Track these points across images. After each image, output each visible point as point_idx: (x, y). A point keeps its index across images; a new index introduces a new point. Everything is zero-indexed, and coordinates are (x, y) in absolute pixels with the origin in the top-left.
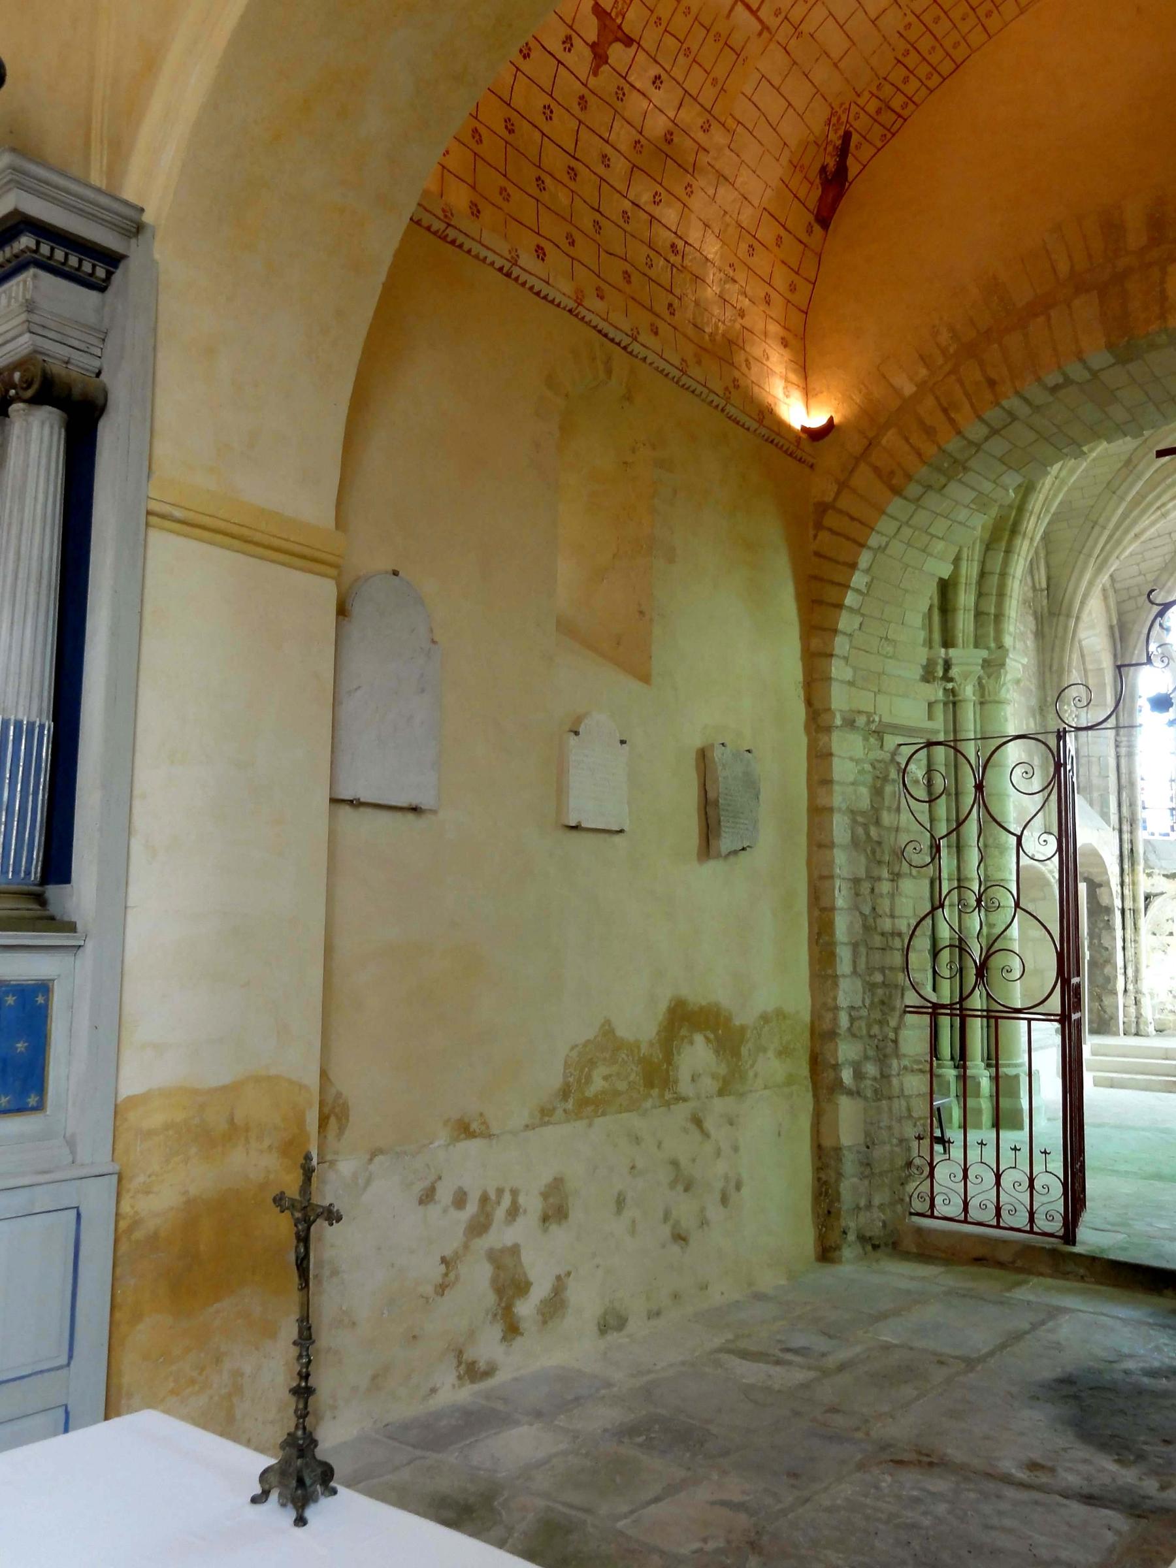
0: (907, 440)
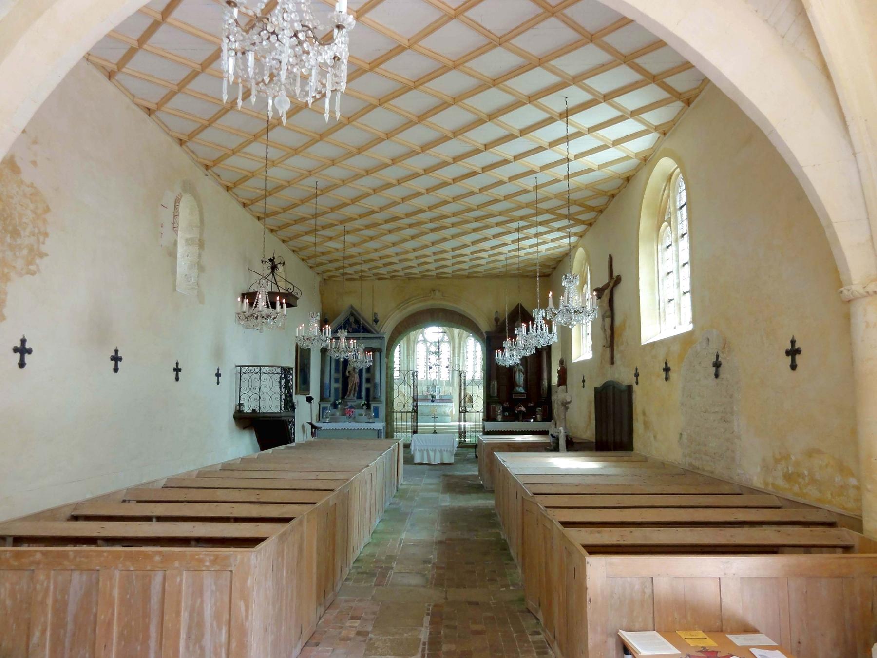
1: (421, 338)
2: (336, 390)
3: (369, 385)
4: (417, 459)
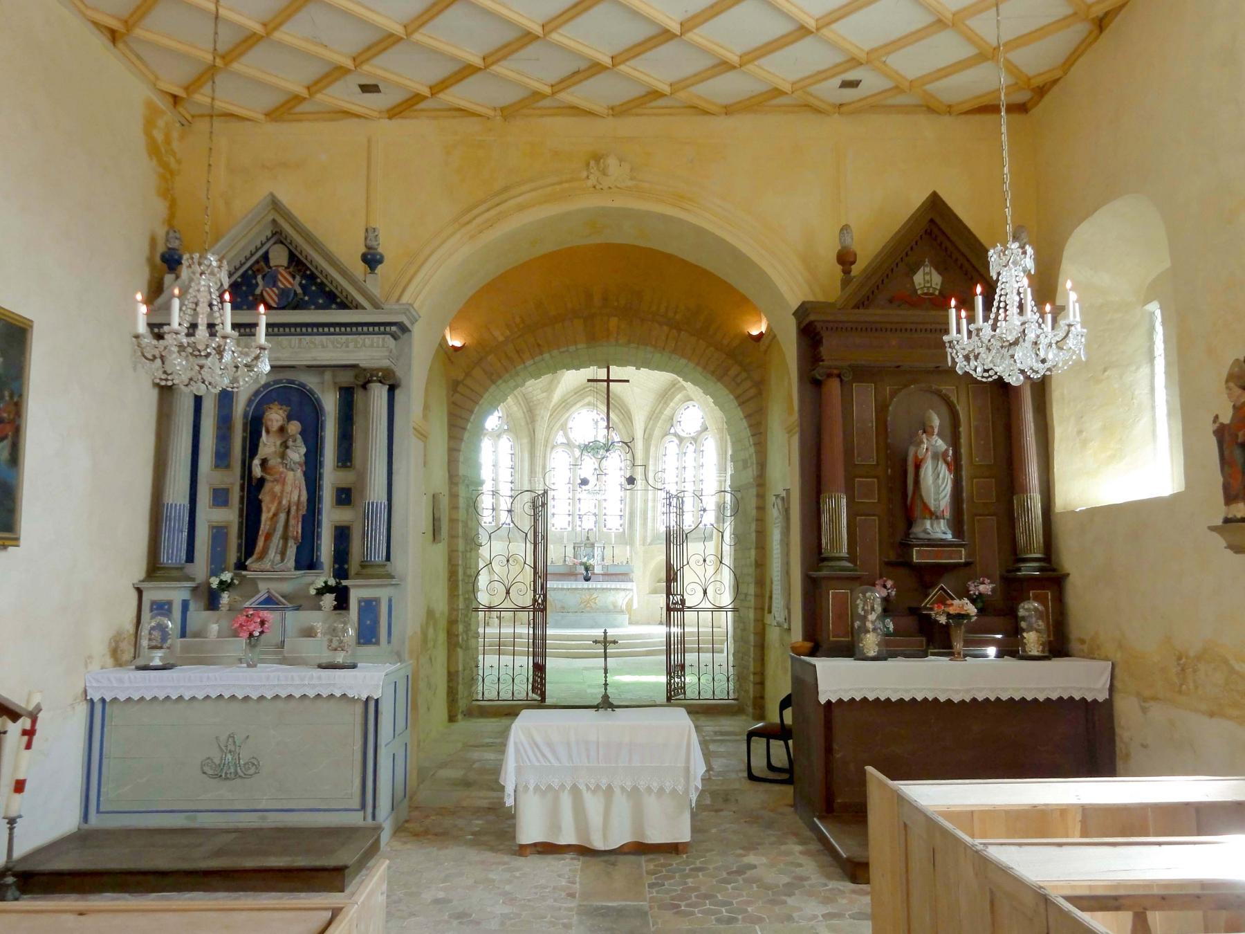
1: (560, 438)
2: (219, 533)
3: (344, 516)
4: (531, 831)
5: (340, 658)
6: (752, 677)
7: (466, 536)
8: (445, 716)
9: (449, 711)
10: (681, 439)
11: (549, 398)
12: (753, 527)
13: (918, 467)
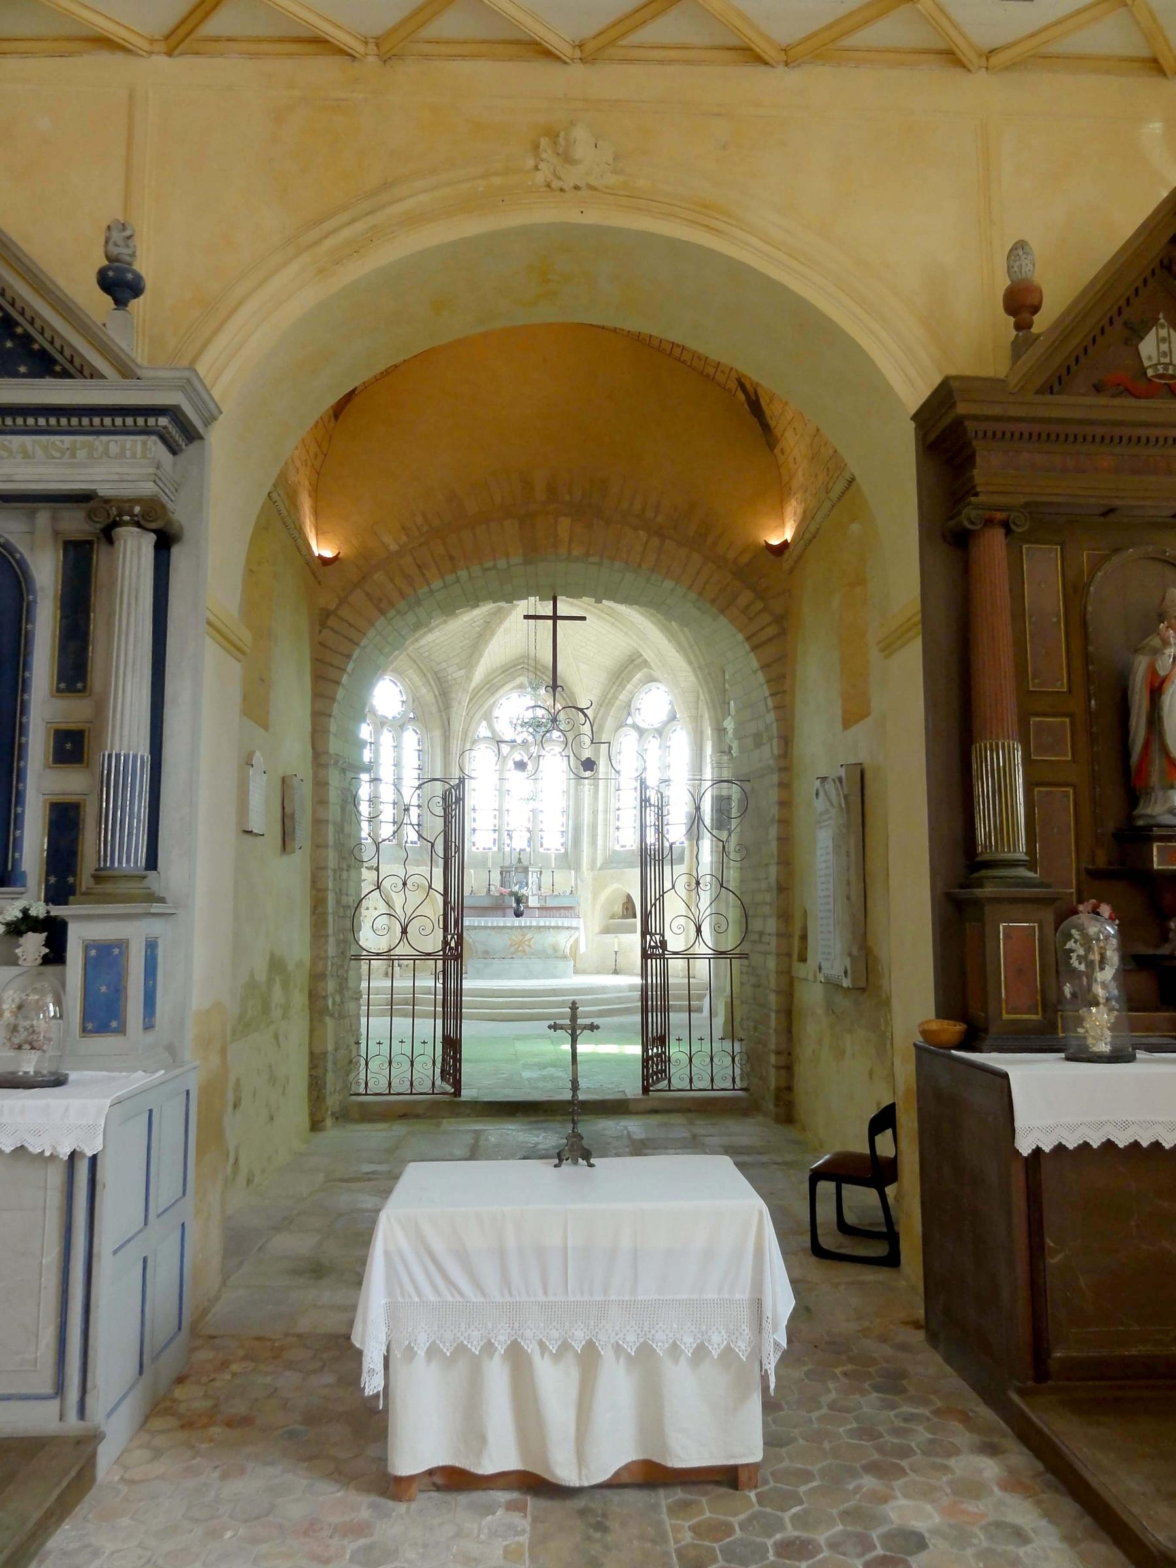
0: (392, 580)
1: (483, 731)
3: (71, 783)
4: (420, 1442)
5: (29, 1064)
6: (773, 1059)
7: (340, 846)
8: (304, 1120)
9: (312, 1115)
10: (641, 732)
11: (468, 678)
12: (773, 832)
13: (1156, 690)
